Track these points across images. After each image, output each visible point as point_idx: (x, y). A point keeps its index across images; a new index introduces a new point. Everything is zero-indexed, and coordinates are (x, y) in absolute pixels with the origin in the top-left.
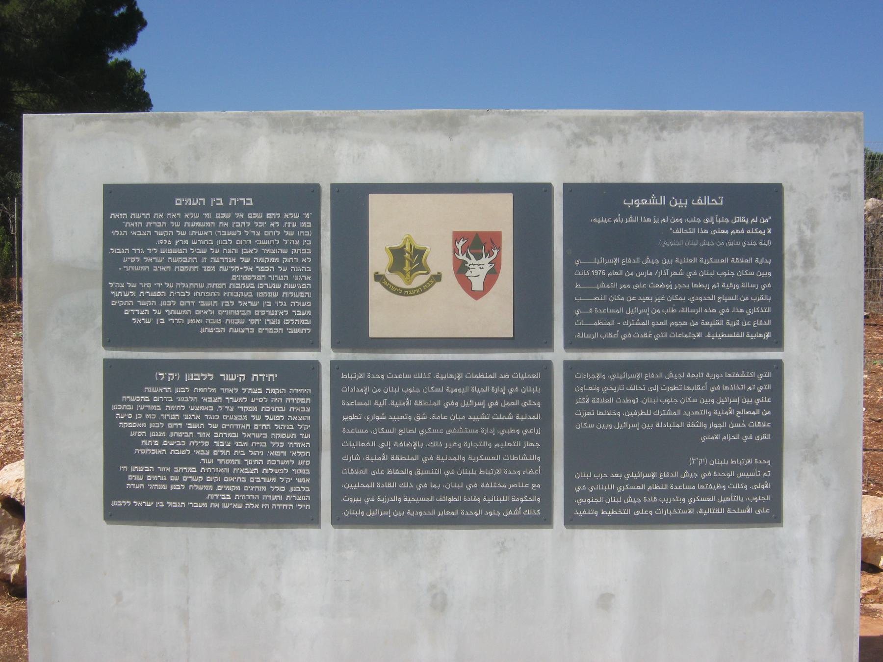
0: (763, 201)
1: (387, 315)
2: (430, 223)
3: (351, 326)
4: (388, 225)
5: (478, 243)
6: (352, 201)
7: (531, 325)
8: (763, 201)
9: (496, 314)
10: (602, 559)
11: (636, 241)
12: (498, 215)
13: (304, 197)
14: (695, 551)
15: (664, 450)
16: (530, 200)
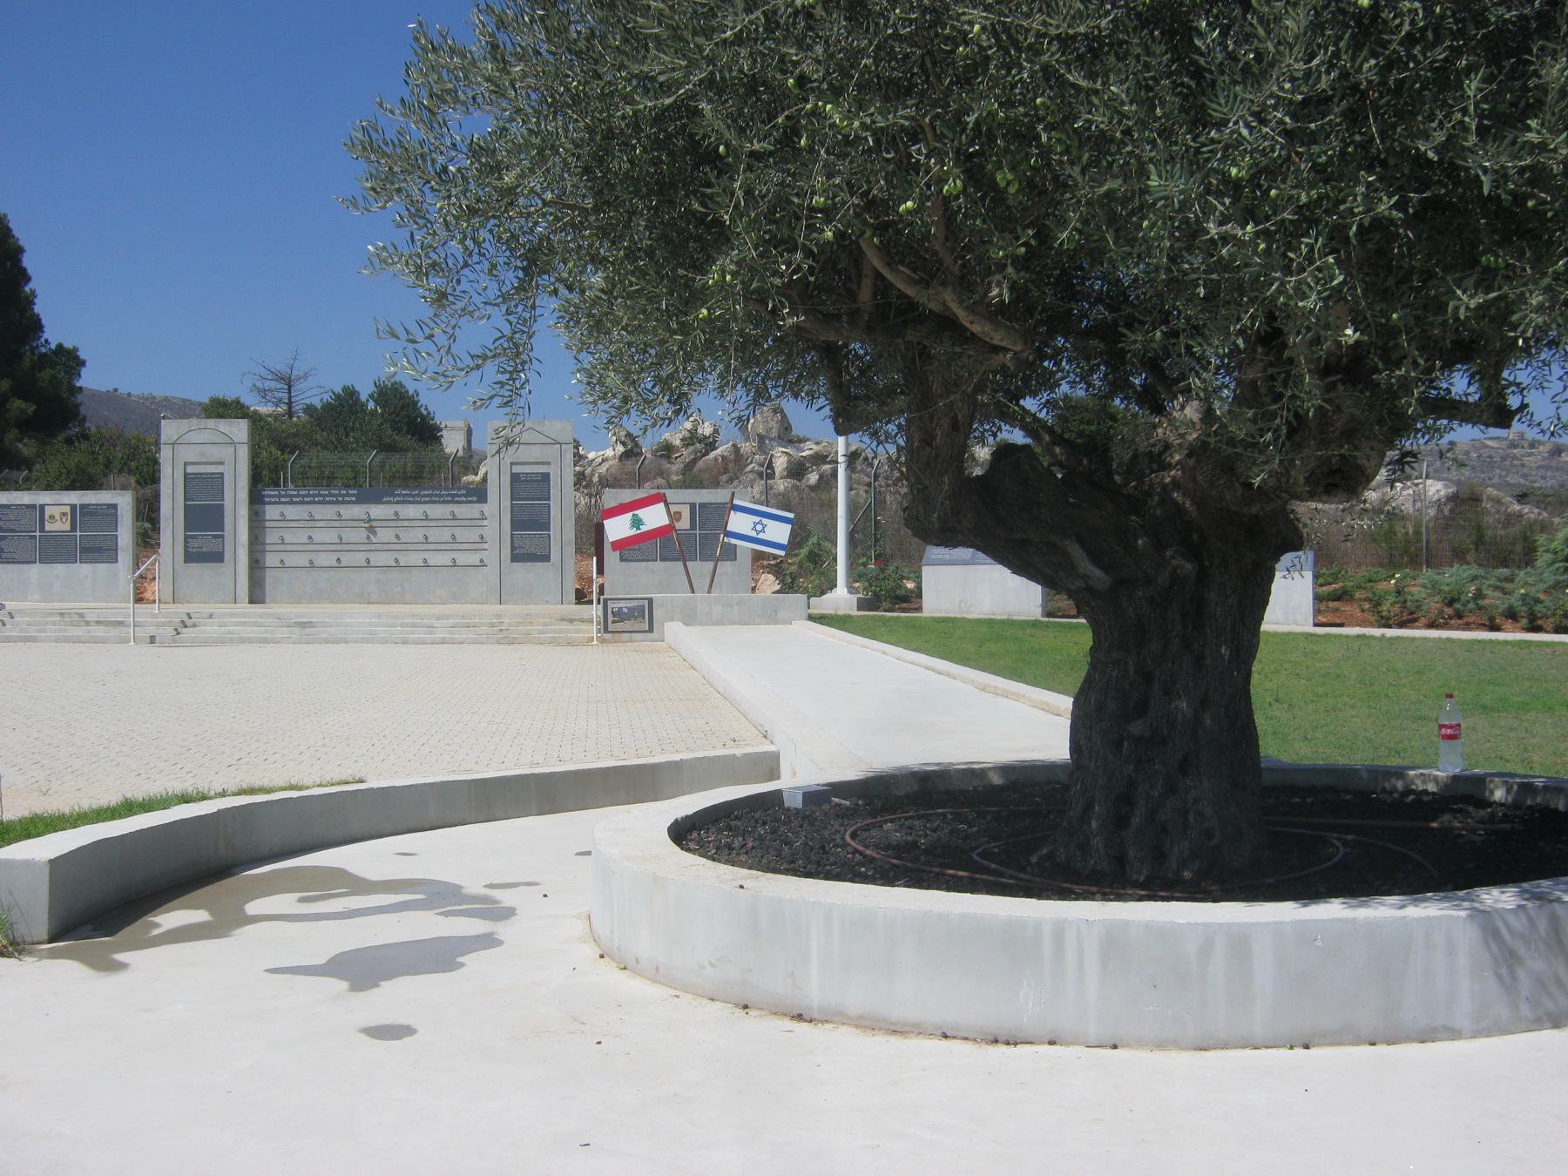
0: (115, 506)
1: (48, 527)
2: (56, 511)
3: (42, 529)
4: (48, 511)
5: (64, 514)
6: (42, 507)
7: (73, 528)
8: (115, 506)
9: (67, 527)
10: (86, 569)
11: (93, 514)
12: (67, 509)
13: (33, 506)
14: (102, 567)
15: (99, 550)
16: (73, 507)
